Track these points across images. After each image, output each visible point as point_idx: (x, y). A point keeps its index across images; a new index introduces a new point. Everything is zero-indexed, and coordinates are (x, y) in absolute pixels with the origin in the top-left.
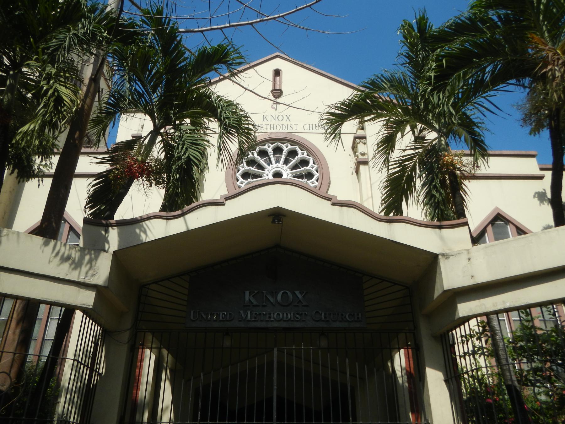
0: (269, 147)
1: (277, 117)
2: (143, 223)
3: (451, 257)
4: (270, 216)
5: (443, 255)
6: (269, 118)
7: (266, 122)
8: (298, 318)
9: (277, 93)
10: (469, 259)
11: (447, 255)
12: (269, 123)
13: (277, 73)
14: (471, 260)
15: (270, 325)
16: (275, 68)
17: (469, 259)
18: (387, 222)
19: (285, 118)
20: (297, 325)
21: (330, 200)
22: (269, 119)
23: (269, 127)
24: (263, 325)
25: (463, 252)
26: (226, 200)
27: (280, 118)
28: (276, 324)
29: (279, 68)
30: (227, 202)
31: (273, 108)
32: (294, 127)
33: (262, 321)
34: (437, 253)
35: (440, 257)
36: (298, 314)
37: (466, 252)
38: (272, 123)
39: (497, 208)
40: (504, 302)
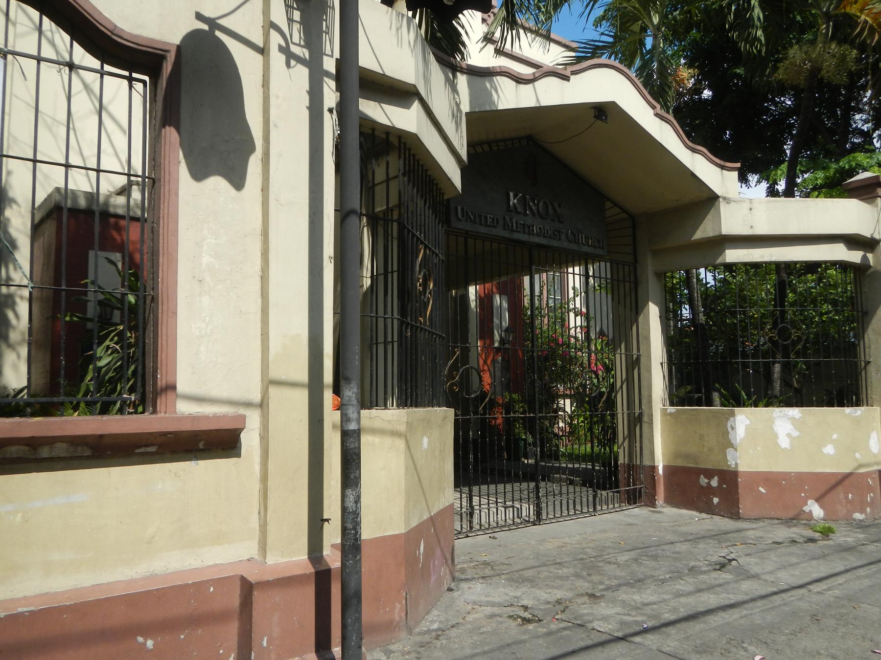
2: (494, 78)
3: (732, 202)
4: (592, 108)
5: (725, 198)
8: (556, 236)
10: (751, 209)
11: (729, 200)
14: (753, 210)
17: (751, 209)
18: (691, 150)
21: (653, 109)
25: (746, 200)
26: (572, 74)
30: (572, 77)
34: (719, 194)
35: (721, 200)
36: (556, 231)
37: (748, 201)
40: (771, 256)
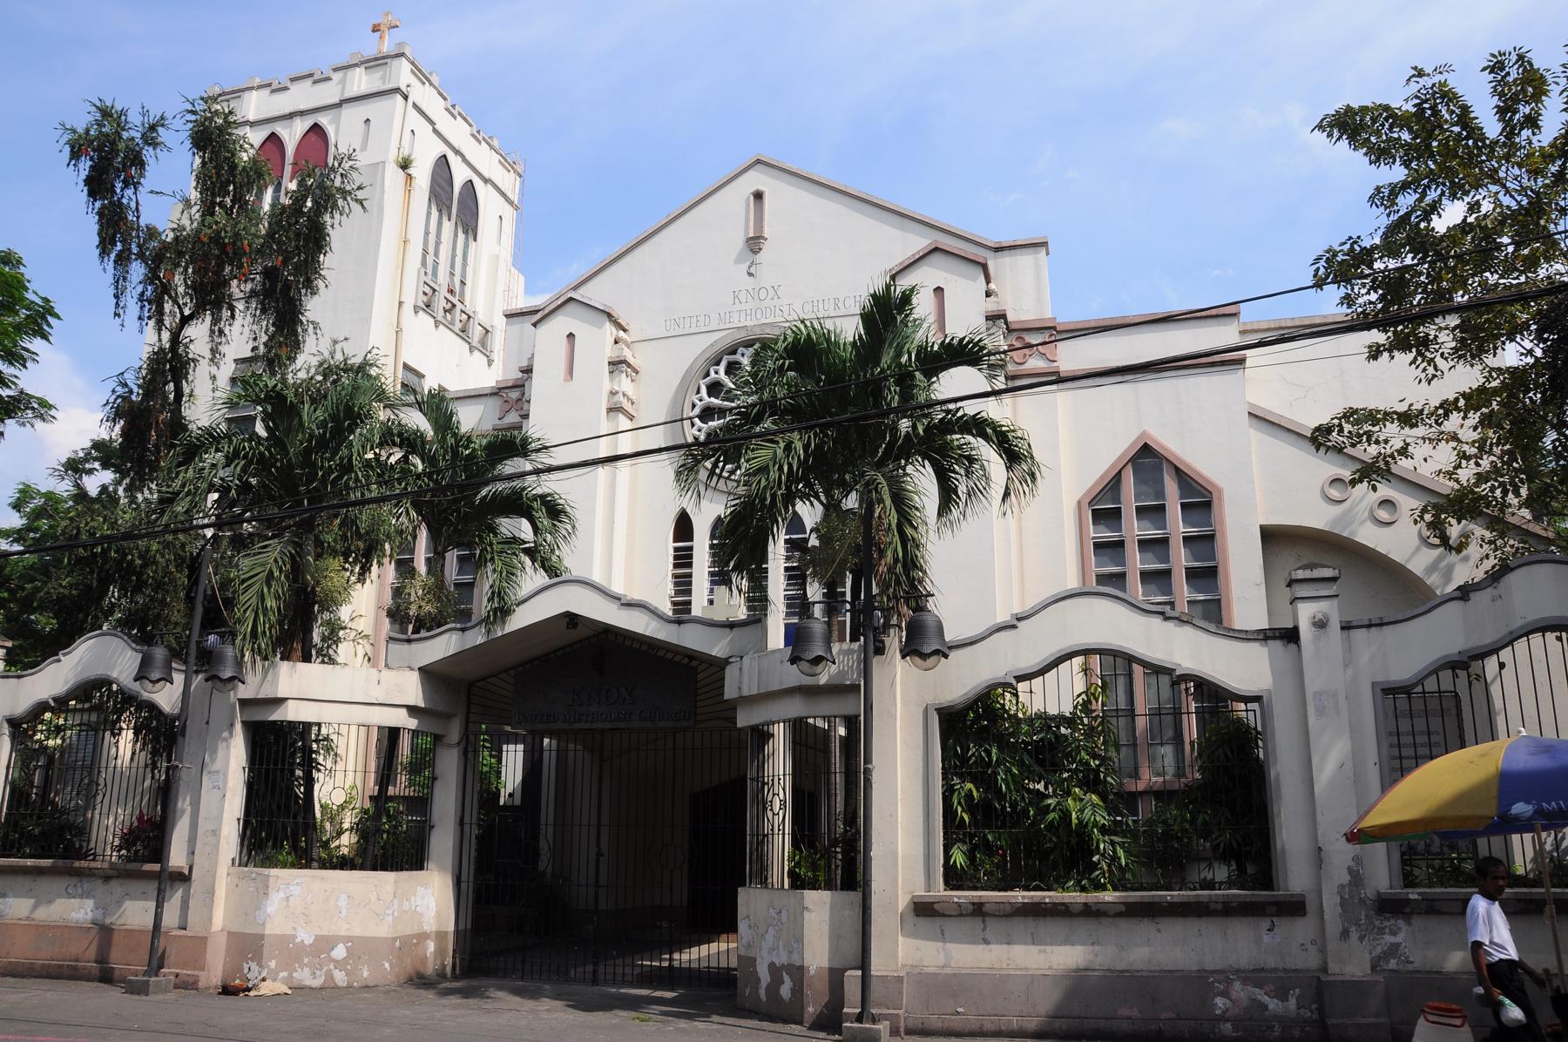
0: (743, 355)
1: (756, 290)
6: (742, 296)
7: (738, 307)
9: (754, 244)
12: (743, 307)
13: (758, 196)
15: (595, 726)
16: (753, 189)
19: (771, 292)
20: (621, 725)
22: (743, 300)
23: (743, 314)
24: (587, 726)
27: (763, 294)
28: (599, 725)
29: (761, 188)
31: (750, 274)
32: (785, 309)
33: (586, 722)
38: (748, 306)
39: (1144, 433)
